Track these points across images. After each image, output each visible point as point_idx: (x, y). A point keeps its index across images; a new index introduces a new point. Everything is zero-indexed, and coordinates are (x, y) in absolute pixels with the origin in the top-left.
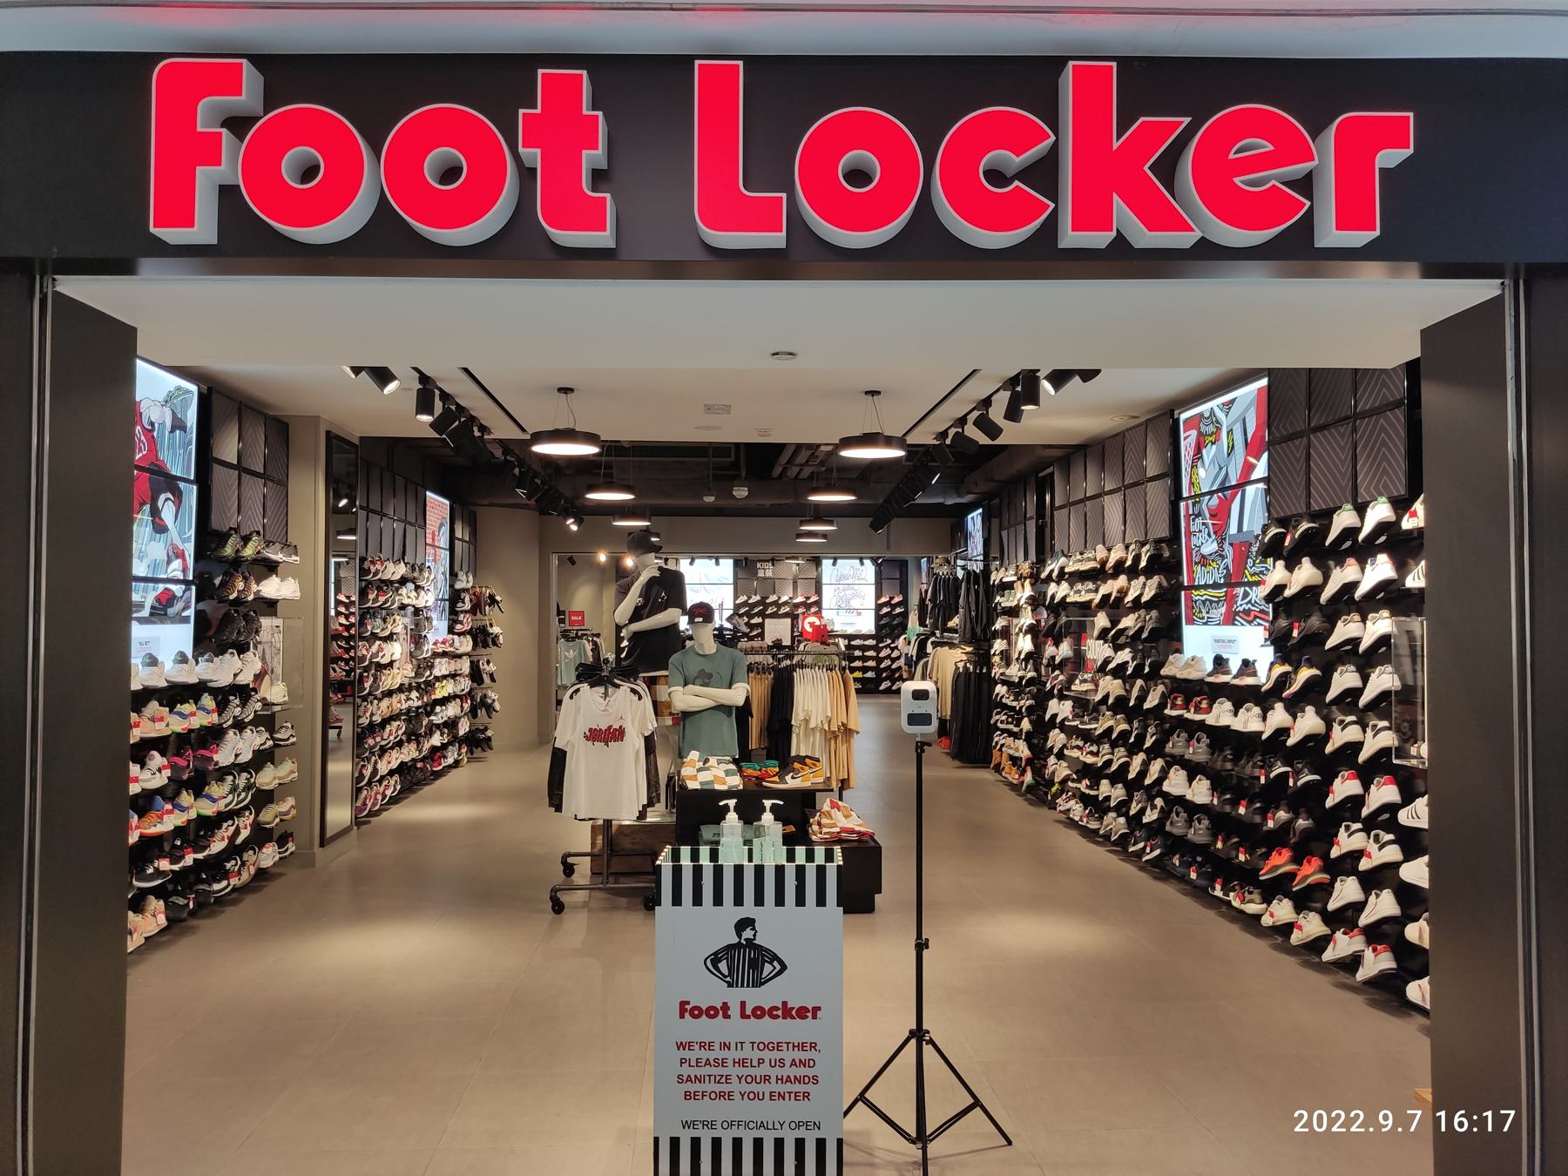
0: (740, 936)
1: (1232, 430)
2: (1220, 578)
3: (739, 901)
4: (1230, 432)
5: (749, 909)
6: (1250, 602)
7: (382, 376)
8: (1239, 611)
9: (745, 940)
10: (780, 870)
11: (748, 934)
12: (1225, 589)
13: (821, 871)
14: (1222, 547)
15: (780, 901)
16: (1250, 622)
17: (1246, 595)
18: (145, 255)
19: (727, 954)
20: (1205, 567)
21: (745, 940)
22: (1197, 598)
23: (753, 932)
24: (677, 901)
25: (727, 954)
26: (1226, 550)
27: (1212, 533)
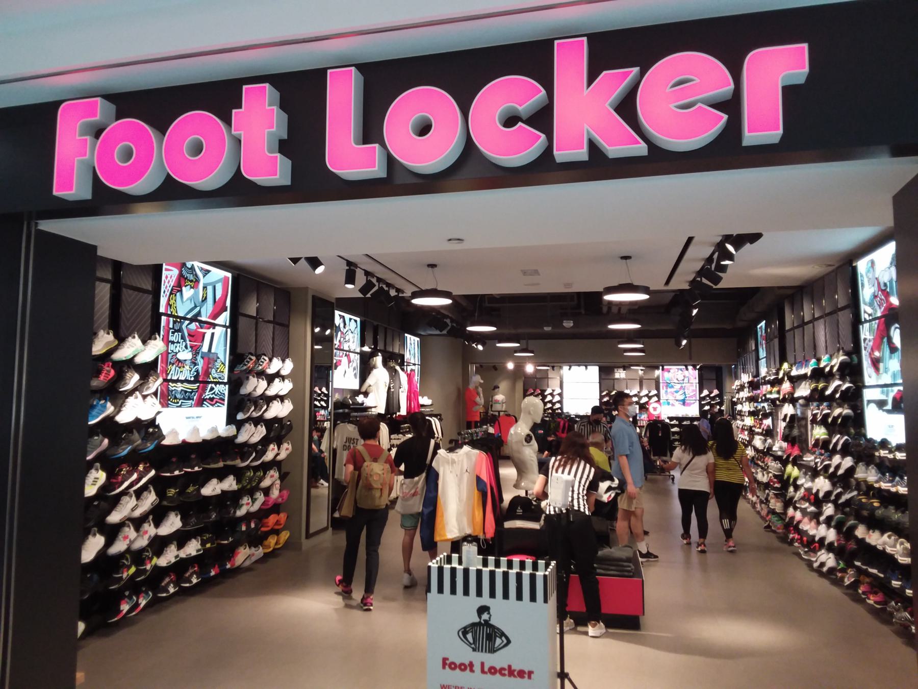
0: (480, 618)
1: (206, 287)
2: (191, 377)
3: (479, 593)
4: (205, 288)
5: (485, 600)
6: (214, 393)
7: (314, 262)
8: (206, 399)
9: (484, 620)
10: (479, 572)
11: (485, 616)
12: (198, 384)
13: (492, 573)
14: (195, 357)
15: (506, 596)
16: (213, 405)
17: (212, 389)
18: (90, 200)
19: (472, 628)
20: (180, 368)
21: (484, 620)
22: (173, 389)
23: (488, 616)
24: (440, 590)
25: (472, 628)
26: (198, 360)
27: (189, 347)
